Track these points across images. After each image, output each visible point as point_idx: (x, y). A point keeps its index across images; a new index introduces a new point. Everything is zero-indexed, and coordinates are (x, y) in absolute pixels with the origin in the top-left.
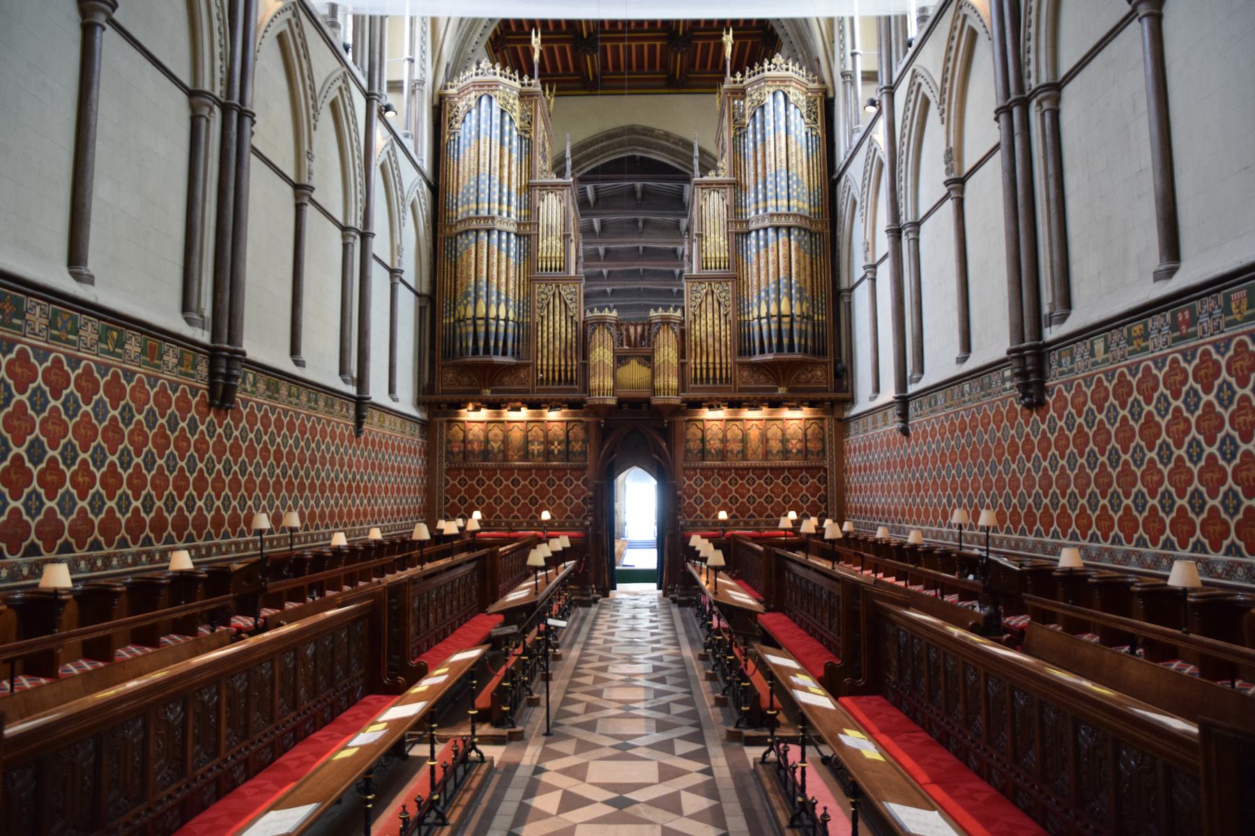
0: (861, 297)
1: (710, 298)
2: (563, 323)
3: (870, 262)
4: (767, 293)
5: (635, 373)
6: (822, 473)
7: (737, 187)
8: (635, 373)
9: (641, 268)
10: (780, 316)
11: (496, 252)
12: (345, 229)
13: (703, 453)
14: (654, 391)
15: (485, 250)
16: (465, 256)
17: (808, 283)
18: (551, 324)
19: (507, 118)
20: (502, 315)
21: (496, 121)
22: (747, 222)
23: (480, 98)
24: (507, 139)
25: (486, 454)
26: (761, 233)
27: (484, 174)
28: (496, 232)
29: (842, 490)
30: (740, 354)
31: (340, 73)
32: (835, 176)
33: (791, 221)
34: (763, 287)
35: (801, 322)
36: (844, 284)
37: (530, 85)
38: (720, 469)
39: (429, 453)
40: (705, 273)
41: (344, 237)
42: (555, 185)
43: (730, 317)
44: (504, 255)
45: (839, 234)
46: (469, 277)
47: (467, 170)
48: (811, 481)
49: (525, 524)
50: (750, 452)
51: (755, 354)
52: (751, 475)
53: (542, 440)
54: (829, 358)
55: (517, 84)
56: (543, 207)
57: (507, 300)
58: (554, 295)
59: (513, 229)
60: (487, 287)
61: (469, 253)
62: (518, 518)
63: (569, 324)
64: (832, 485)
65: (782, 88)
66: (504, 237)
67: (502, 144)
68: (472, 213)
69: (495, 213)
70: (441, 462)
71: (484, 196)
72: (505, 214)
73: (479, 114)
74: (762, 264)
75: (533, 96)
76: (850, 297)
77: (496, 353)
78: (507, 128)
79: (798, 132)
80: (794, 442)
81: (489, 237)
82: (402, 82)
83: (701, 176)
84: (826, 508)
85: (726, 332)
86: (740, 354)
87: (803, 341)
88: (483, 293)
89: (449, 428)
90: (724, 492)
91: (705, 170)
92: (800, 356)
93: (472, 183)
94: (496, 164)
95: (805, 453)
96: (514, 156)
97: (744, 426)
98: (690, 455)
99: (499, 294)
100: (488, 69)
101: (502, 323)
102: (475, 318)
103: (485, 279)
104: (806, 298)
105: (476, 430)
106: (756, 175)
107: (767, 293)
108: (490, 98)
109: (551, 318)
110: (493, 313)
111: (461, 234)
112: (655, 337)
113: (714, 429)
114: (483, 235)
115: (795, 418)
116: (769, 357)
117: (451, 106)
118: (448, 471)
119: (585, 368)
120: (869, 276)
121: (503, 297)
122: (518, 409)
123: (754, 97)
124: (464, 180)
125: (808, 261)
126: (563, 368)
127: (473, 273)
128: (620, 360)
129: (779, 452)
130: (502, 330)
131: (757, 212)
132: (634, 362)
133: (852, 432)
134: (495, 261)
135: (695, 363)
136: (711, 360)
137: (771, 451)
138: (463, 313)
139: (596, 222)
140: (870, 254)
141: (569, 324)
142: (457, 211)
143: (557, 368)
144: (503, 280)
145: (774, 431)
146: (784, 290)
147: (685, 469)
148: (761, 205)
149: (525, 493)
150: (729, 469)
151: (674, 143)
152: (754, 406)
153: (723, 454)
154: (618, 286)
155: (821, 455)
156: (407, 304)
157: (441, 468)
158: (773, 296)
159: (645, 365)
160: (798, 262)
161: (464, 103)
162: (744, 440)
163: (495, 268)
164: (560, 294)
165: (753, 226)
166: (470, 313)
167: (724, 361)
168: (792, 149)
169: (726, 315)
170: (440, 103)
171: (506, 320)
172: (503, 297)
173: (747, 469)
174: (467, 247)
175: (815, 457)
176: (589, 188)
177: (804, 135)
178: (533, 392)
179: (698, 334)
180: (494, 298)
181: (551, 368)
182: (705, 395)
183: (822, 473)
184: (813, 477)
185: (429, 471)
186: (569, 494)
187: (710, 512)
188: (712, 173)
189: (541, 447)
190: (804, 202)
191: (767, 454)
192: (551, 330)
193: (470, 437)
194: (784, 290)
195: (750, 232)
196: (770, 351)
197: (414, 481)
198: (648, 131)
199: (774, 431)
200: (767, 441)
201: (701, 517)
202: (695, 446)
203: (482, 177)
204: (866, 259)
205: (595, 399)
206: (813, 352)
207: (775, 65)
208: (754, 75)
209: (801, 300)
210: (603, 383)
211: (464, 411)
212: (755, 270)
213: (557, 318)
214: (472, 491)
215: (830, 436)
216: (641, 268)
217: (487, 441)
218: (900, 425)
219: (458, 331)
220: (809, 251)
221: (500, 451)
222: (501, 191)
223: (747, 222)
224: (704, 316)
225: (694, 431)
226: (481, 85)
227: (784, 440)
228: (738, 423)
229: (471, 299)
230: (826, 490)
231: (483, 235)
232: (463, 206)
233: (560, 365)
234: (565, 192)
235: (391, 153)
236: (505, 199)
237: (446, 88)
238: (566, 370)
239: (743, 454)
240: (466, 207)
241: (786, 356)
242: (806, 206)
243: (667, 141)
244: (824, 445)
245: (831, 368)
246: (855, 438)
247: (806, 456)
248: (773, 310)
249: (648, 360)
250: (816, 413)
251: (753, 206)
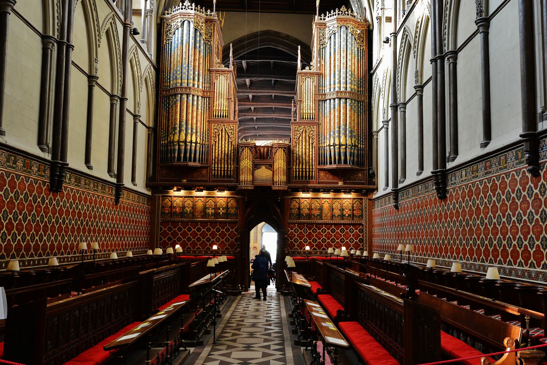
0: (382, 135)
1: (304, 134)
2: (227, 145)
3: (385, 119)
4: (334, 132)
5: (263, 173)
6: (361, 227)
7: (320, 75)
9: (274, 107)
10: (340, 145)
11: (191, 107)
13: (299, 215)
15: (185, 105)
16: (174, 108)
17: (356, 128)
18: (220, 145)
19: (198, 34)
20: (194, 141)
21: (192, 35)
22: (325, 95)
23: (184, 21)
24: (198, 45)
25: (183, 214)
26: (332, 101)
27: (185, 64)
28: (191, 96)
29: (371, 236)
30: (319, 164)
31: (111, 15)
32: (372, 72)
33: (348, 95)
34: (332, 129)
35: (351, 148)
36: (375, 129)
37: (211, 15)
38: (308, 224)
39: (152, 213)
40: (302, 121)
41: (111, 100)
42: (223, 71)
43: (314, 144)
44: (195, 108)
45: (373, 102)
46: (176, 119)
47: (176, 61)
48: (355, 231)
49: (203, 252)
50: (324, 215)
51: (327, 164)
52: (324, 227)
53: (214, 207)
54: (366, 167)
55: (204, 15)
56: (217, 82)
57: (196, 132)
58: (222, 130)
59: (200, 94)
60: (186, 125)
61: (176, 106)
62: (200, 248)
63: (230, 146)
64: (366, 233)
65: (345, 24)
66: (195, 98)
67: (195, 48)
68: (179, 85)
69: (191, 85)
70: (158, 218)
71: (185, 76)
72: (196, 86)
73: (183, 31)
74: (332, 118)
75: (212, 22)
76: (377, 135)
77: (190, 160)
78: (198, 39)
79: (353, 48)
80: (347, 210)
81: (187, 98)
82: (141, 10)
83: (302, 70)
84: (363, 246)
85: (313, 153)
86: (319, 164)
87: (352, 158)
88: (184, 128)
89: (163, 200)
90: (310, 236)
91: (303, 68)
92: (350, 166)
93: (178, 68)
94: (191, 59)
95: (352, 216)
96: (202, 54)
97: (321, 202)
98: (292, 216)
99: (192, 129)
100: (188, 6)
101: (194, 144)
102: (179, 141)
103: (185, 121)
104: (354, 136)
105: (178, 201)
106: (330, 70)
107: (334, 132)
108: (189, 22)
109: (220, 142)
110: (189, 139)
111: (172, 95)
112: (275, 154)
113: (305, 204)
114: (185, 96)
115: (347, 198)
116: (334, 166)
117: (167, 25)
118: (162, 223)
119: (237, 170)
120: (385, 126)
121: (194, 131)
122: (202, 191)
123: (331, 28)
124: (174, 67)
125: (356, 116)
126: (226, 169)
127: (178, 117)
128: (256, 166)
129: (339, 215)
130: (193, 148)
131: (330, 90)
132: (263, 167)
133: (376, 206)
134: (190, 111)
135: (296, 168)
136: (304, 167)
137: (335, 215)
138: (172, 138)
139: (248, 81)
140: (386, 115)
141: (230, 146)
142: (170, 82)
143: (223, 169)
144: (195, 121)
145: (336, 205)
146: (342, 131)
147: (289, 223)
148: (332, 86)
149: (204, 235)
150: (312, 224)
151: (291, 41)
152: (326, 191)
153: (309, 216)
154: (261, 116)
155: (361, 218)
156: (142, 133)
157: (158, 221)
158: (337, 134)
159: (269, 169)
160: (350, 117)
161: (175, 24)
163: (190, 115)
164: (225, 130)
165: (328, 97)
166: (176, 138)
167: (311, 167)
168: (349, 57)
169: (312, 144)
170: (161, 22)
171: (196, 143)
172: (194, 131)
173: (322, 224)
174: (176, 103)
175: (358, 219)
176: (244, 63)
177: (356, 49)
178: (210, 182)
179: (298, 153)
180: (189, 131)
181: (219, 169)
182: (300, 185)
183: (361, 227)
184: (356, 229)
185: (151, 223)
186: (227, 236)
187: (302, 246)
188: (307, 68)
189: (213, 211)
190: (354, 85)
191: (333, 216)
192: (220, 149)
193: (175, 205)
194: (342, 131)
195: (326, 100)
196: (335, 163)
197: (143, 228)
199: (336, 205)
200: (333, 209)
201: (297, 249)
202: (295, 211)
203: (184, 66)
204: (384, 118)
205: (243, 186)
206: (358, 164)
207: (342, 11)
208: (331, 16)
209: (351, 137)
210: (245, 177)
211: (172, 191)
212: (328, 121)
213: (223, 143)
214: (175, 234)
215: (366, 208)
216: (274, 107)
217: (184, 207)
218: (394, 204)
219: (169, 148)
220: (357, 111)
221: (190, 213)
222: (194, 73)
223: (325, 95)
224: (300, 144)
225: (295, 204)
226: (184, 15)
227: (342, 210)
228: (317, 200)
229: (177, 131)
230: (363, 236)
231: (185, 96)
232: (173, 80)
233: (224, 168)
234: (229, 75)
235: (135, 53)
236: (196, 78)
237: (164, 14)
238: (227, 171)
239: (320, 216)
240: (175, 81)
241: (343, 166)
242: (356, 87)
243: (288, 40)
244: (362, 212)
245: (366, 172)
246: (377, 210)
247: (353, 218)
248: (337, 142)
249: (271, 166)
250: (358, 195)
251: (328, 87)
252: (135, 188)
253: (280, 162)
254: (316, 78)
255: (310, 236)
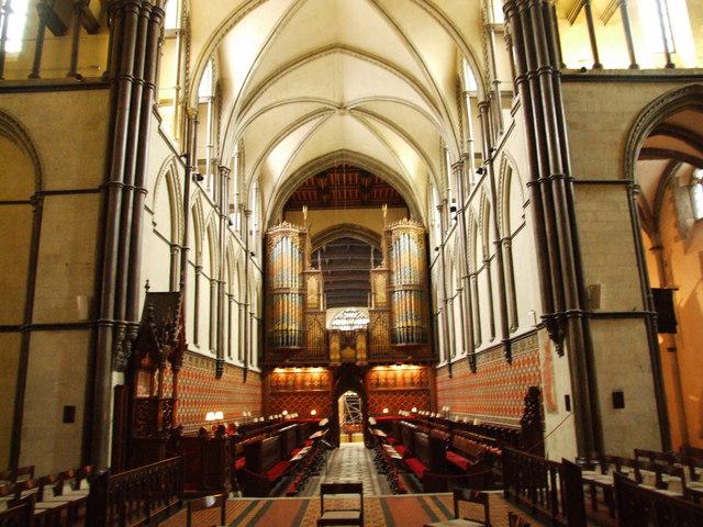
5: (349, 352)
7: (390, 272)
8: (349, 352)
12: (240, 304)
14: (357, 360)
39: (264, 386)
71: (285, 279)
85: (386, 334)
115: (414, 370)
116: (404, 344)
119: (328, 351)
128: (343, 347)
153: (386, 385)
156: (255, 322)
162: (395, 378)
191: (405, 384)
198: (352, 226)
205: (332, 364)
210: (335, 356)
214: (281, 403)
217: (287, 381)
241: (410, 344)
249: (354, 347)
252: (231, 362)
253: (361, 344)
254: (386, 274)
255: (387, 401)
